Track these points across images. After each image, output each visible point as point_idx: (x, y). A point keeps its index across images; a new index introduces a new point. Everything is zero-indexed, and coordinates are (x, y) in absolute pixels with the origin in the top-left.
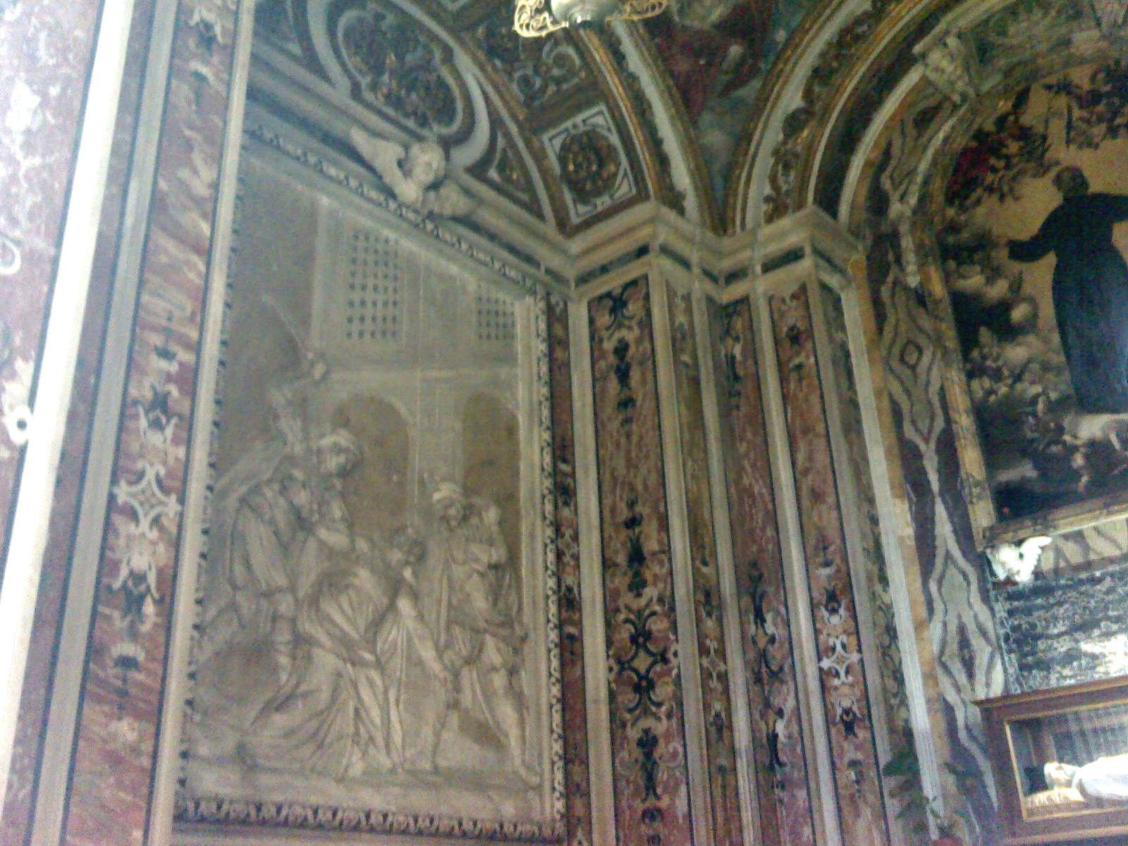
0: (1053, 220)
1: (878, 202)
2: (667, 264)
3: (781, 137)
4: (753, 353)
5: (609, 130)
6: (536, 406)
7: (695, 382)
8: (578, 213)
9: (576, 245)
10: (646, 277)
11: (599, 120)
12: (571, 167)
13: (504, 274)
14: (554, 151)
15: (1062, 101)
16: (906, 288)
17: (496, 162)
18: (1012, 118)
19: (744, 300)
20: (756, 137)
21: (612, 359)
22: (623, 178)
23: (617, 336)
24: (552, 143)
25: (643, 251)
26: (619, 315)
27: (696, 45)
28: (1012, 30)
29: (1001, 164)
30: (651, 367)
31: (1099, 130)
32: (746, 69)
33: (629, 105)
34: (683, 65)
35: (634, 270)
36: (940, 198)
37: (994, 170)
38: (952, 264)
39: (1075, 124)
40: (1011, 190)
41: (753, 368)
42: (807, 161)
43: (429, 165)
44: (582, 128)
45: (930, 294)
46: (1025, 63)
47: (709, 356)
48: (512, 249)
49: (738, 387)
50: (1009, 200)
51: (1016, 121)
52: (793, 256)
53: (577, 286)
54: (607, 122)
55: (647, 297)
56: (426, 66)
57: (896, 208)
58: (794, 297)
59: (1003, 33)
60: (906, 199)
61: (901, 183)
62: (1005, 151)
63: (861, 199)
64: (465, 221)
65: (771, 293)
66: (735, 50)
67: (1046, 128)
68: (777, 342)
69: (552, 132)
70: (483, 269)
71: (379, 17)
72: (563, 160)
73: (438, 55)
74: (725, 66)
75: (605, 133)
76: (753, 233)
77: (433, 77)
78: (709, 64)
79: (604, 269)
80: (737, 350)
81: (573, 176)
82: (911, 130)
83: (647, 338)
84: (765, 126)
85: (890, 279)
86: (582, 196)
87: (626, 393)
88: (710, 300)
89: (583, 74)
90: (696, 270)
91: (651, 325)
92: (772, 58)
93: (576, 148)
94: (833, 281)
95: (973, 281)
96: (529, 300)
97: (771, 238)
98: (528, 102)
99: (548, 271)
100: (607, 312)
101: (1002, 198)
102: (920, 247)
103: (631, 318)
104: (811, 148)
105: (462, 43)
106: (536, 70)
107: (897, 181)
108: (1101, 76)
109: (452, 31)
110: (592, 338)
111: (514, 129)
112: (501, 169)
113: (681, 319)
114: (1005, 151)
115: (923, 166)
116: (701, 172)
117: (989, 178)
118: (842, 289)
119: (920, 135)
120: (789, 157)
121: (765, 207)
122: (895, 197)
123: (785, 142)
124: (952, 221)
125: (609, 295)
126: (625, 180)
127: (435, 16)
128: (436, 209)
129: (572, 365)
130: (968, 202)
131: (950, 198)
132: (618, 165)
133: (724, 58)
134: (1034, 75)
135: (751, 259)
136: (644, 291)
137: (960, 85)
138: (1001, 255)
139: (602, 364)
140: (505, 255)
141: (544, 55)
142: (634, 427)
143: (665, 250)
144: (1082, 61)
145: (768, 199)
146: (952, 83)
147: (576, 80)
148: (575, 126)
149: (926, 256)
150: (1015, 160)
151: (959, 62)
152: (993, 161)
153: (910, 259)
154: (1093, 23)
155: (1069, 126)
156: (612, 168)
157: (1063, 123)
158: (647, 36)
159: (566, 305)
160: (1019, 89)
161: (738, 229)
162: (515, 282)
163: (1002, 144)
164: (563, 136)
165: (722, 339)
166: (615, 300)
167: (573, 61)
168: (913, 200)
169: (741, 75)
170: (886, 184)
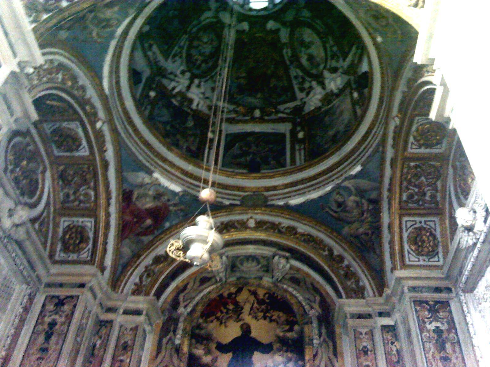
0: (236, 340)
1: (175, 304)
2: (89, 295)
3: (151, 262)
4: (105, 347)
5: (91, 229)
6: (5, 336)
7: (78, 351)
8: (60, 255)
9: (55, 269)
10: (78, 297)
11: (89, 224)
12: (67, 236)
13: (22, 272)
14: (63, 226)
15: (252, 298)
16: (173, 343)
17: (40, 221)
18: (234, 296)
19: (110, 322)
20: (142, 258)
21: (46, 327)
22: (87, 251)
23: (54, 317)
24: (65, 222)
25: (82, 286)
26: (58, 308)
27: (136, 213)
28: (245, 264)
29: (225, 311)
30: (63, 338)
31: (261, 315)
32: (149, 231)
33: (104, 225)
34: (128, 218)
35: (74, 292)
36: (198, 313)
37: (222, 312)
38: (194, 341)
39: (254, 308)
40: (225, 322)
41: (102, 353)
42: (158, 276)
43: (21, 217)
44: (80, 224)
45: (182, 349)
46: (245, 278)
47: (87, 342)
48: (29, 262)
49: (92, 359)
50: (223, 325)
51: (235, 297)
52: (137, 312)
53: (45, 287)
54: (91, 227)
55: (75, 306)
56: (34, 172)
57: (181, 310)
58: (132, 329)
59: (242, 264)
60: (187, 307)
61: (187, 300)
62: (228, 306)
63: (169, 300)
64: (19, 244)
65: (122, 324)
66: (149, 222)
67: (244, 305)
68: (117, 345)
69: (66, 219)
70: (14, 266)
71: (28, 144)
72: (65, 232)
73: (41, 169)
74: (142, 225)
75: (88, 230)
76: (127, 295)
77: (35, 177)
78: (137, 222)
79: (61, 285)
80: (99, 342)
81: (66, 240)
82: (198, 283)
83: (67, 324)
84: (147, 255)
85: (168, 337)
86: (66, 249)
87: (46, 345)
88: (97, 317)
89: (92, 204)
90: (97, 302)
91: (71, 320)
92: (160, 231)
93: (74, 230)
94: (148, 328)
95: (199, 351)
96: (24, 286)
97: (133, 302)
98: (63, 202)
99: (37, 276)
100: (54, 304)
101: (221, 323)
102: (184, 329)
103: (63, 312)
104: (161, 273)
105: (52, 169)
106: (75, 193)
107: (185, 299)
108: (267, 295)
109: (51, 164)
110: (41, 312)
111: (52, 210)
112: (41, 224)
113: (84, 321)
114: (228, 306)
115: (198, 298)
116: (115, 261)
117: (219, 314)
118: (149, 333)
119: (200, 285)
120: (151, 272)
121: (133, 287)
122: (182, 304)
123: (152, 265)
124: (200, 324)
125: (58, 297)
126: (87, 253)
127: (48, 154)
128: (12, 235)
129: (26, 322)
130: (209, 319)
131: (202, 315)
132: (87, 245)
133: (143, 223)
134: (247, 284)
135: (121, 306)
136: (75, 302)
137: (221, 275)
138: (213, 346)
139: (40, 327)
140: (26, 264)
141: (81, 189)
142: (43, 362)
143: (92, 290)
144: (263, 287)
145: (136, 284)
146: (219, 273)
147: (88, 205)
148: (78, 221)
149: (186, 333)
150: (230, 312)
151: (224, 266)
152: (222, 308)
153: (180, 332)
154: (271, 276)
155: (252, 309)
156: (85, 245)
157: (250, 306)
158: (121, 201)
159: (36, 293)
160: (240, 286)
161: (120, 292)
162: (24, 277)
163: (228, 304)
164: (70, 223)
165: (94, 336)
166: (59, 300)
167: (91, 197)
168: (189, 309)
169: (147, 231)
170: (181, 298)
